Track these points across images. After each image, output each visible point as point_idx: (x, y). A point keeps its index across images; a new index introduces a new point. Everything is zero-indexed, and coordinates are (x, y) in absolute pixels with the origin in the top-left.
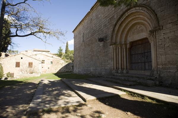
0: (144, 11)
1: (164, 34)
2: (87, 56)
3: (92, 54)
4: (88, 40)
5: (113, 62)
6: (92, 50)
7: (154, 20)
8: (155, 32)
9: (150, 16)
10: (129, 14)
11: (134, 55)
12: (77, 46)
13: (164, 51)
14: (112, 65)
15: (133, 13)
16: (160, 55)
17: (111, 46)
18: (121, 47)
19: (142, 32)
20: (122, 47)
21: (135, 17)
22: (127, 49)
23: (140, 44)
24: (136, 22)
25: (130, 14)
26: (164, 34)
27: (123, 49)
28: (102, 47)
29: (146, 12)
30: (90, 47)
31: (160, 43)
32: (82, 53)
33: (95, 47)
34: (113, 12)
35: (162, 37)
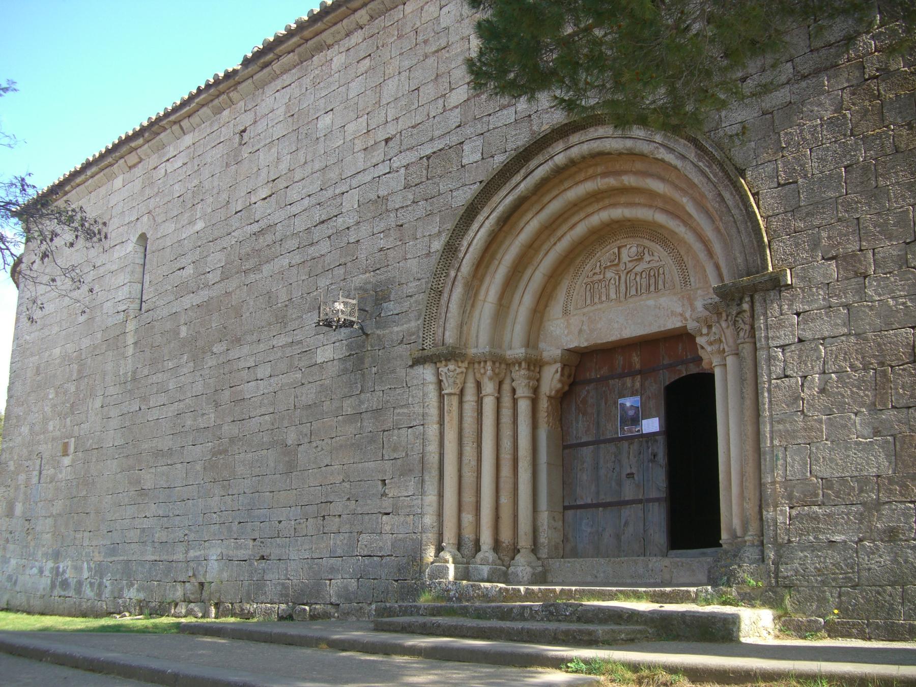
0: (683, 157)
2: (166, 443)
3: (228, 430)
4: (189, 301)
5: (431, 498)
6: (226, 395)
7: (742, 228)
8: (747, 299)
9: (720, 195)
10: (575, 152)
11: (587, 451)
12: (57, 351)
14: (422, 515)
15: (609, 154)
17: (419, 369)
18: (500, 383)
19: (657, 289)
20: (506, 387)
21: (612, 181)
22: (544, 404)
23: (640, 372)
24: (617, 213)
25: (584, 158)
27: (515, 401)
28: (333, 369)
29: (696, 166)
30: (210, 362)
32: (114, 412)
33: (262, 372)
34: (454, 118)
35: (786, 336)
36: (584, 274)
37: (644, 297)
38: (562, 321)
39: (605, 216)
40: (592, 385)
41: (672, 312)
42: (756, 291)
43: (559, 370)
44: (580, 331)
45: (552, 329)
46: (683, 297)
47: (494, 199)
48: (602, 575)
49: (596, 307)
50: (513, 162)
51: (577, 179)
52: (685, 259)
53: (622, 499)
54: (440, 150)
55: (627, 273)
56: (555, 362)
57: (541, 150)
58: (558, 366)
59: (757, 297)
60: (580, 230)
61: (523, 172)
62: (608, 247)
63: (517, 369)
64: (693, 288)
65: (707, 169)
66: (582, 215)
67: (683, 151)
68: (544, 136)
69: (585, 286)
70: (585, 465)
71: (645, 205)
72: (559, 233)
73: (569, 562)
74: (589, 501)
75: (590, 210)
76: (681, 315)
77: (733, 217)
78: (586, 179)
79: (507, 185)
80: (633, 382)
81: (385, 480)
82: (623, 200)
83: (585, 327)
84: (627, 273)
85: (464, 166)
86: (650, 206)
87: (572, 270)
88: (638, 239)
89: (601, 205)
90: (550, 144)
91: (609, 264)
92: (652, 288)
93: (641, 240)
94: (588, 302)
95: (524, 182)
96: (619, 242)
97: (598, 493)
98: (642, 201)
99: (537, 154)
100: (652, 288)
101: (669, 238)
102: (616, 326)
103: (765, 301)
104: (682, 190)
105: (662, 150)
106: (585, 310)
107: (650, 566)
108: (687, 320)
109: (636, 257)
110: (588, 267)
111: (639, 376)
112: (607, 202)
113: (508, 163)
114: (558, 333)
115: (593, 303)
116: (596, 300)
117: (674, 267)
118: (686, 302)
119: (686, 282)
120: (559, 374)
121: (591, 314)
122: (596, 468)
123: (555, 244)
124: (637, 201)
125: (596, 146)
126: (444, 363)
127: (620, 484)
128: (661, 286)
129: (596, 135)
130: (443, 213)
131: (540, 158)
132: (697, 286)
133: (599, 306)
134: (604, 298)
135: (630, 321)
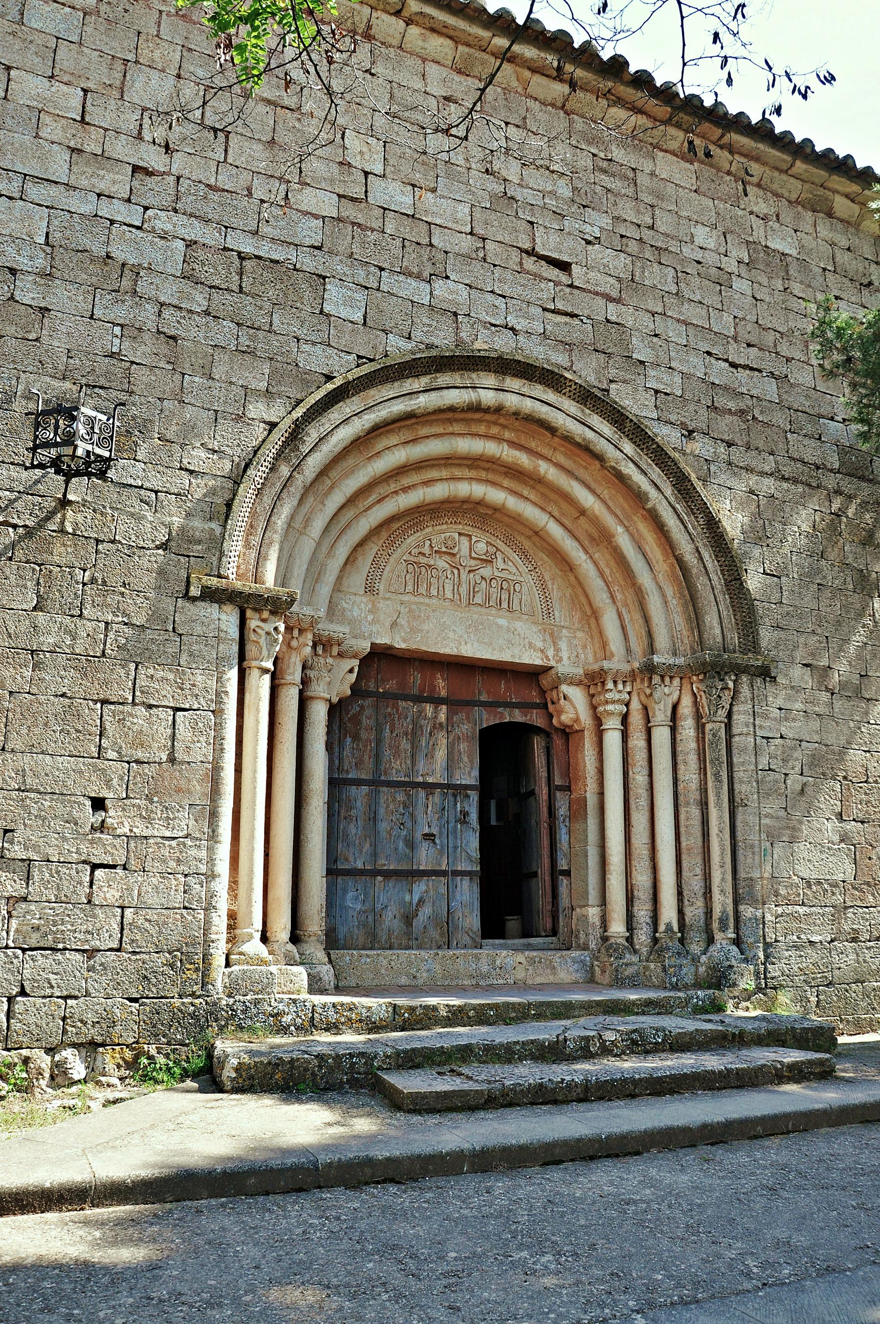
1: (780, 709)
8: (733, 677)
13: (782, 813)
16: (764, 836)
17: (211, 610)
24: (496, 496)
26: (780, 709)
31: (763, 762)
36: (404, 546)
37: (493, 611)
38: (365, 600)
39: (478, 490)
40: (369, 701)
41: (530, 644)
42: (743, 672)
43: (356, 670)
44: (394, 624)
45: (345, 605)
46: (545, 631)
47: (372, 392)
48: (425, 975)
49: (421, 600)
50: (424, 361)
51: (474, 429)
52: (549, 584)
53: (414, 868)
54: (272, 261)
55: (470, 571)
56: (355, 657)
57: (462, 370)
58: (356, 663)
59: (744, 678)
60: (438, 492)
61: (424, 381)
62: (444, 527)
63: (320, 652)
64: (558, 624)
65: (686, 518)
66: (444, 473)
67: (658, 483)
68: (484, 357)
69: (404, 564)
70: (353, 812)
71: (535, 504)
72: (406, 481)
73: (368, 956)
74: (360, 865)
75: (457, 472)
76: (542, 651)
77: (710, 581)
78: (486, 437)
79: (396, 384)
80: (436, 711)
81: (103, 800)
82: (506, 483)
83: (402, 621)
84: (470, 571)
85: (328, 316)
86: (543, 509)
87: (384, 535)
88: (488, 535)
89: (473, 474)
90: (478, 370)
91: (444, 549)
92: (505, 605)
93: (494, 538)
94: (410, 588)
95: (426, 395)
96: (461, 526)
97: (375, 855)
98: (532, 497)
99: (454, 370)
100: (505, 605)
101: (531, 552)
102: (451, 635)
103: (752, 686)
104: (617, 516)
105: (631, 465)
106: (406, 598)
107: (498, 963)
108: (549, 660)
109: (484, 557)
110: (411, 540)
111: (444, 707)
112: (483, 474)
113: (420, 358)
114: (355, 614)
115: (415, 593)
116: (422, 590)
117: (535, 589)
118: (548, 637)
119: (549, 612)
120: (353, 677)
121: (414, 607)
122: (373, 819)
123: (396, 492)
124: (525, 493)
125: (544, 411)
126: (266, 614)
127: (411, 845)
128: (516, 607)
129: (544, 397)
130: (279, 365)
131: (455, 378)
132: (562, 624)
133: (427, 600)
134: (434, 592)
135: (472, 635)
